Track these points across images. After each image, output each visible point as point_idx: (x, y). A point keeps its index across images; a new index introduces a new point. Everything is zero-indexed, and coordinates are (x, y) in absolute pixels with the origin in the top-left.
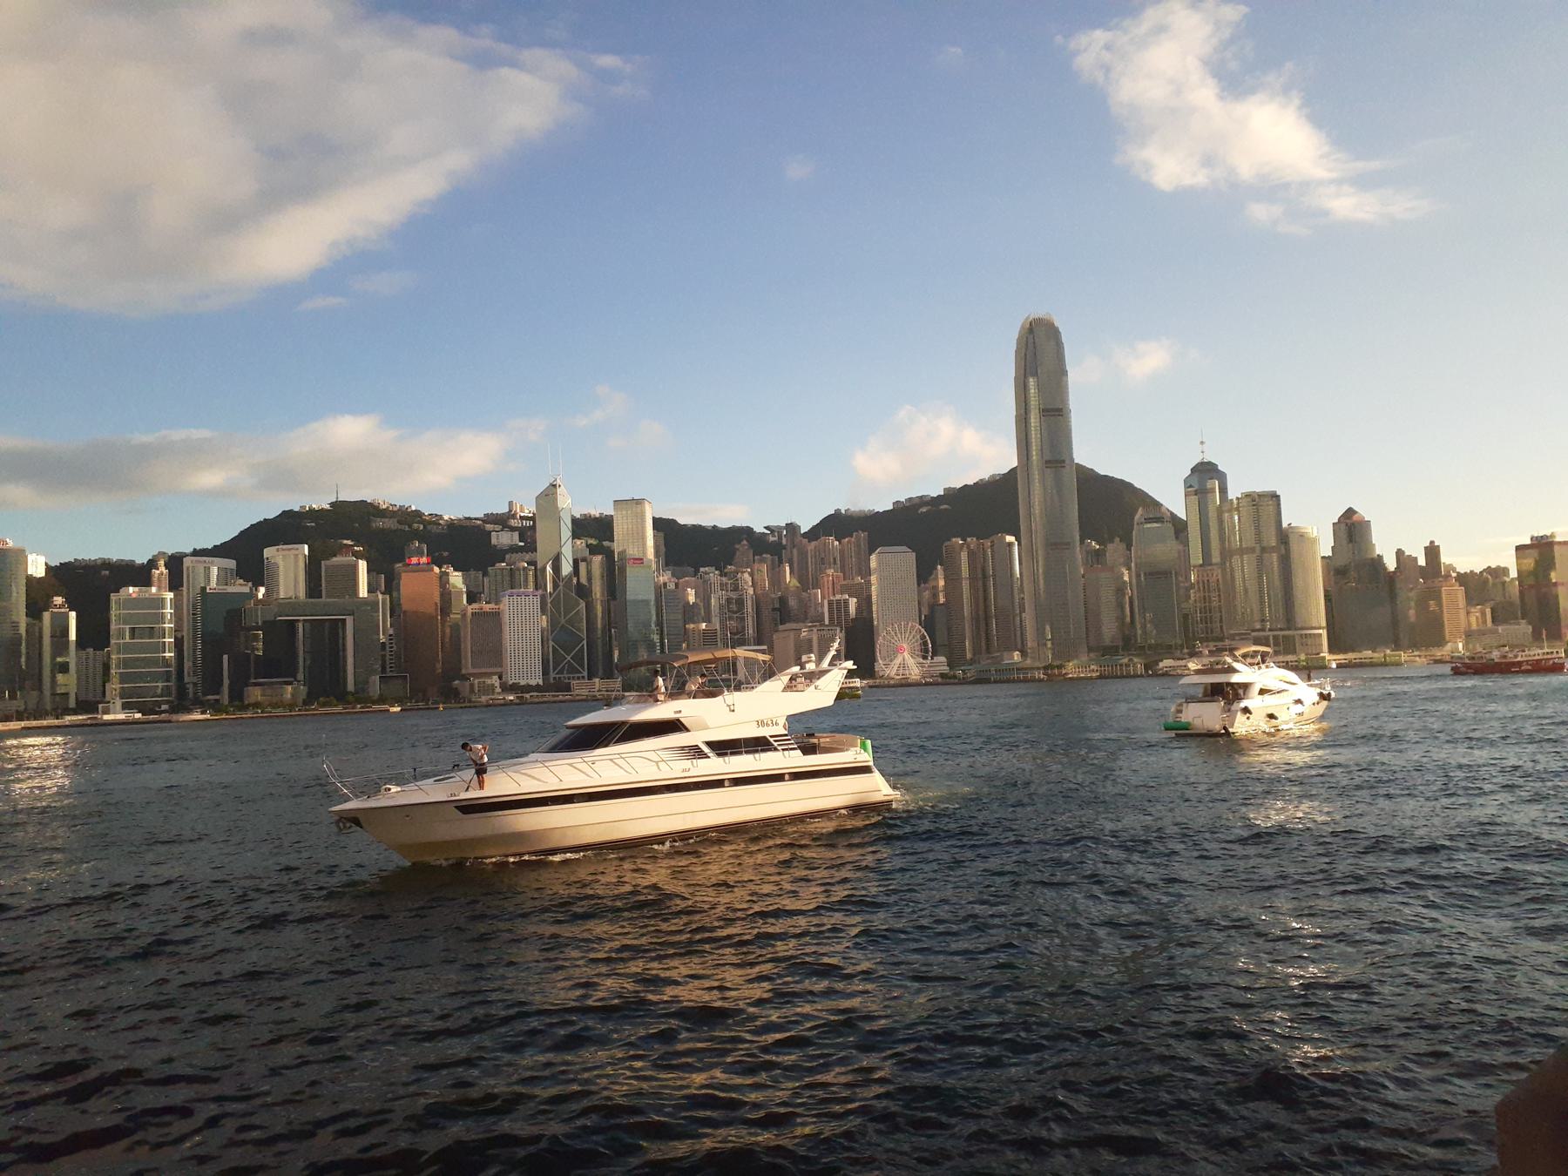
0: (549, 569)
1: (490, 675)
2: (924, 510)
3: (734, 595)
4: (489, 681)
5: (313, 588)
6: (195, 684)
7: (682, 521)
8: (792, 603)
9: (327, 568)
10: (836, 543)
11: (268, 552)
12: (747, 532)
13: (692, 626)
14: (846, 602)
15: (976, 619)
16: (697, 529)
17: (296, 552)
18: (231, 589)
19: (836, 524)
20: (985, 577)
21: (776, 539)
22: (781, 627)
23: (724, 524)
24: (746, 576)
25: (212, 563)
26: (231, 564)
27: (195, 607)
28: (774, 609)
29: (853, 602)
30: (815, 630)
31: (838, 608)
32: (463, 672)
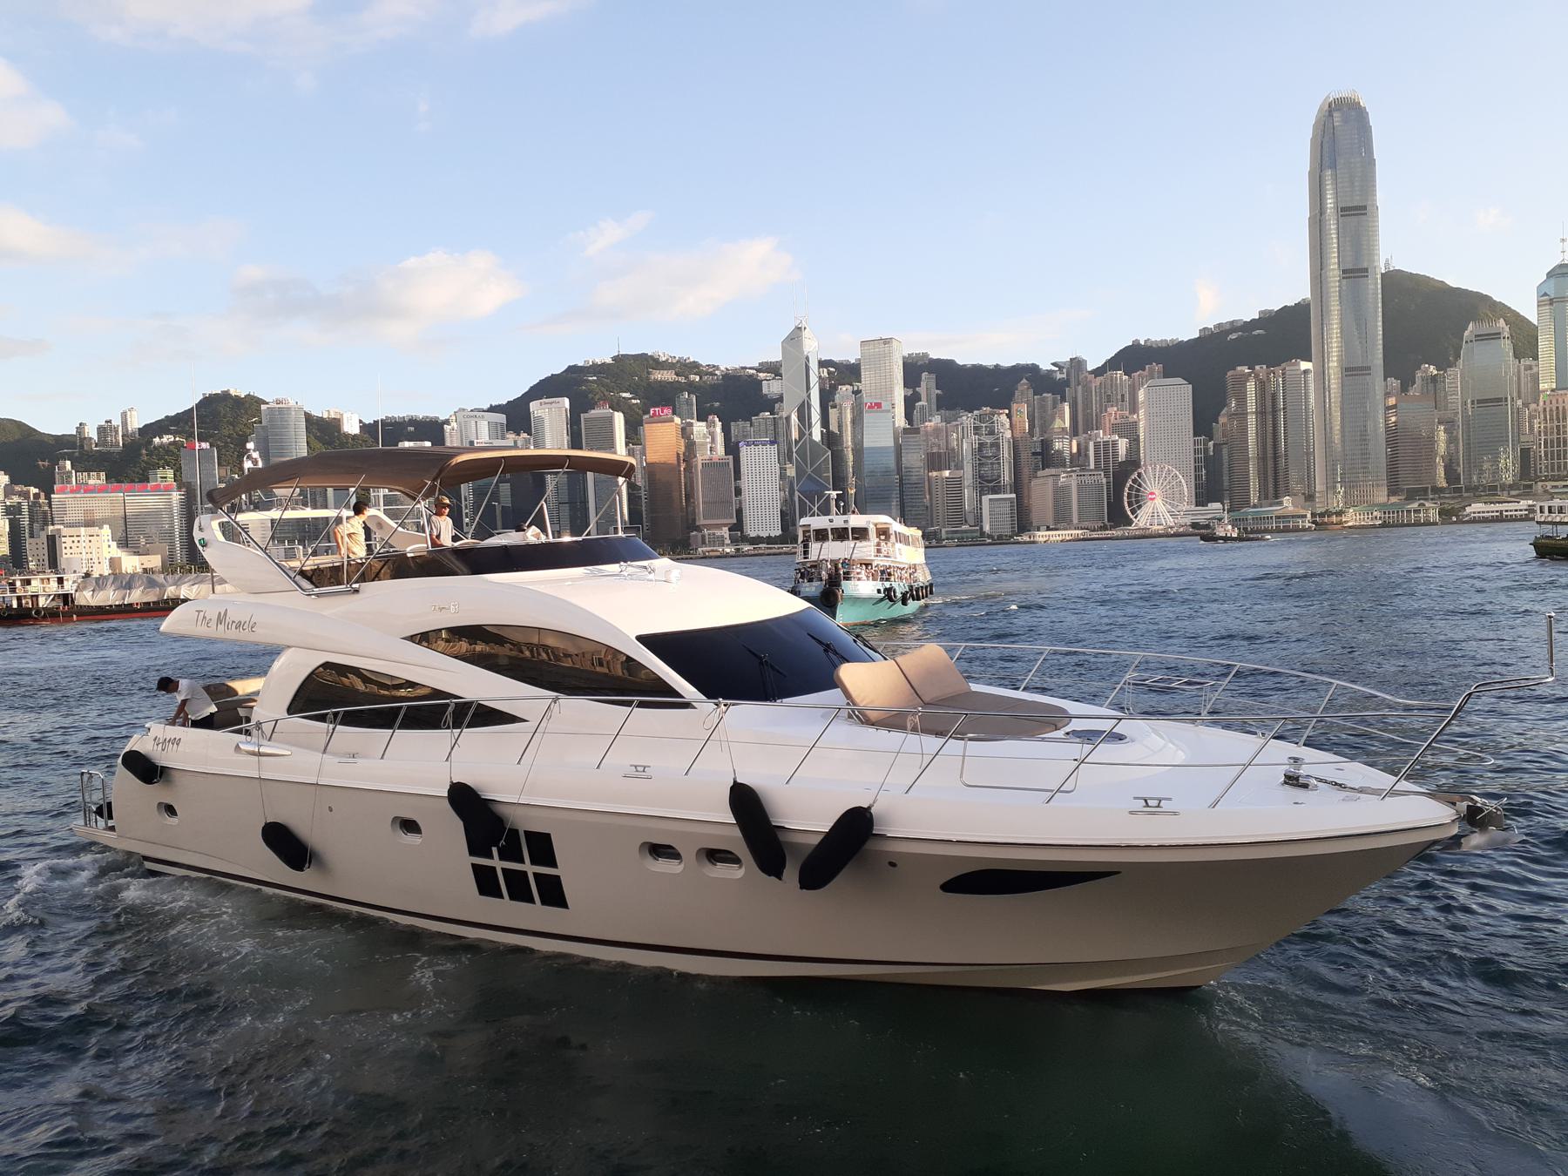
0: (794, 418)
1: (719, 526)
2: (1233, 336)
3: (989, 440)
7: (960, 362)
9: (586, 420)
10: (1125, 377)
12: (1033, 369)
13: (935, 474)
14: (1115, 444)
15: (1262, 458)
16: (978, 370)
19: (1134, 358)
20: (1275, 411)
21: (1064, 376)
22: (1040, 473)
23: (1007, 363)
24: (1004, 418)
28: (1034, 454)
29: (1123, 445)
31: (1106, 449)
32: (697, 524)
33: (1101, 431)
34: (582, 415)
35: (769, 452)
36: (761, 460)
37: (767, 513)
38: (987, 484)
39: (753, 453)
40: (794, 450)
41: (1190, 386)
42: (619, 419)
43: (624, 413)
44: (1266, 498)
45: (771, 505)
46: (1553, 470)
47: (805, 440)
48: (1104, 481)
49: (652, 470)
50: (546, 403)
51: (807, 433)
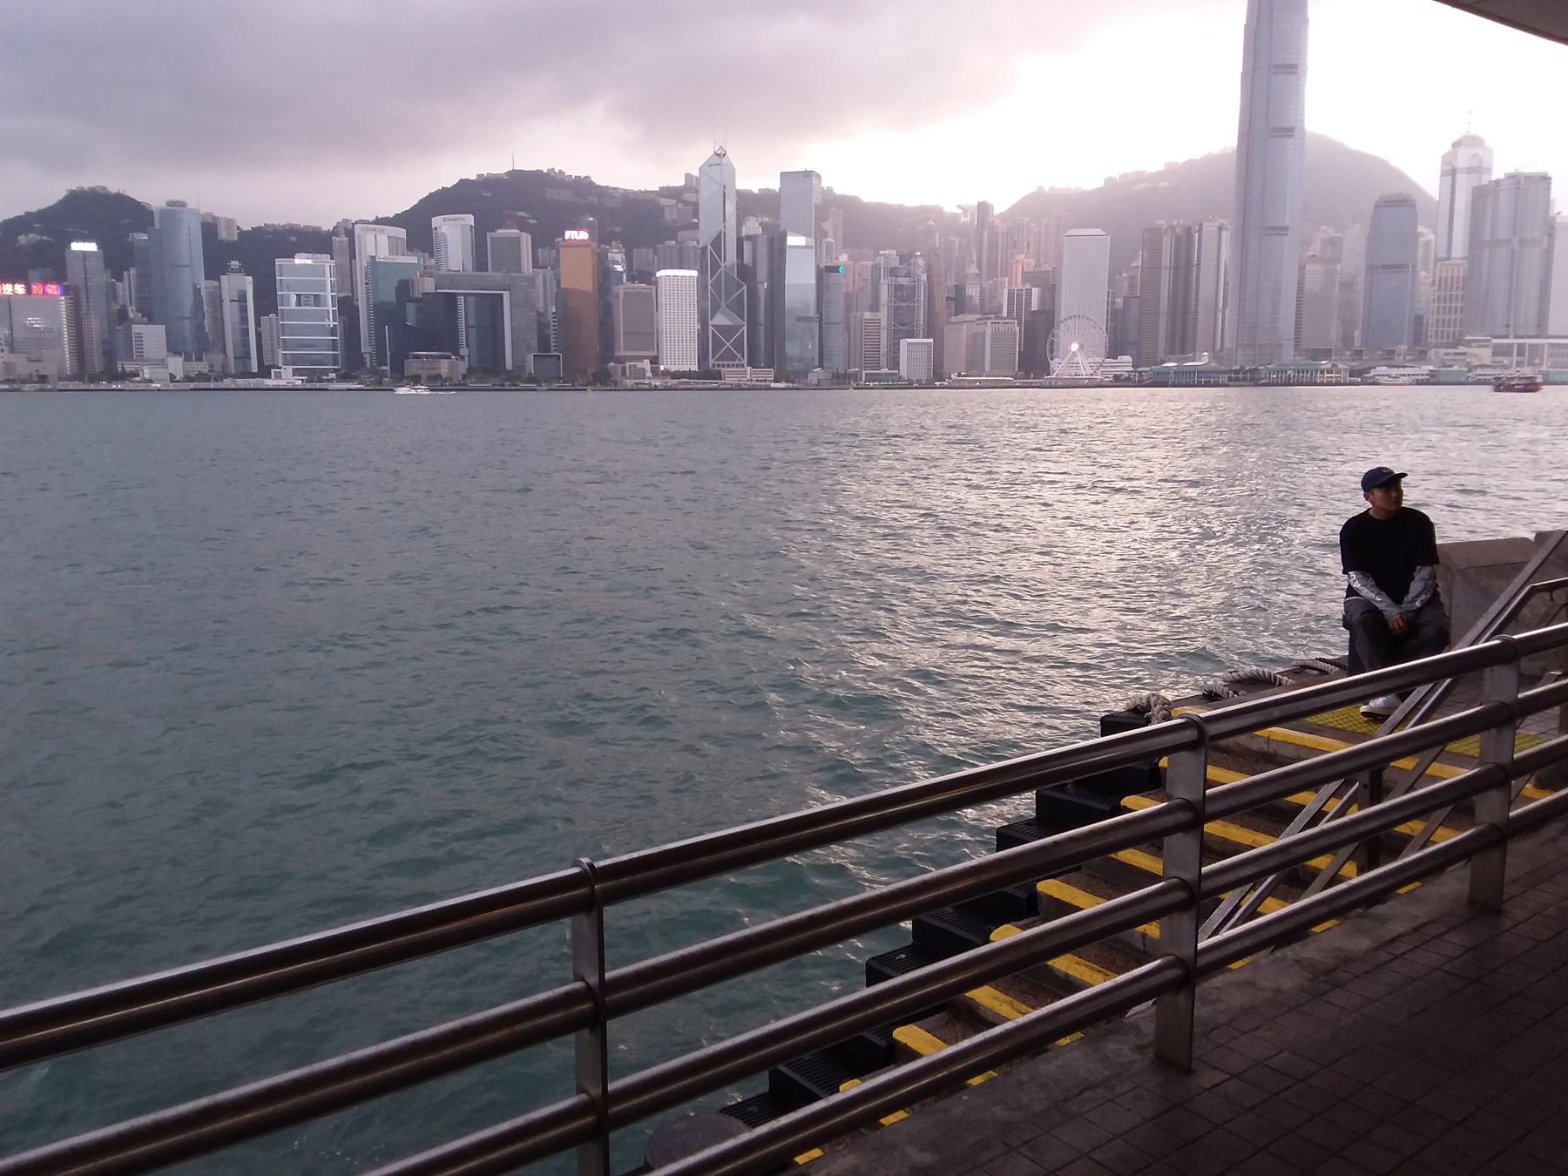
3: (903, 281)
4: (639, 365)
5: (480, 263)
6: (370, 353)
8: (973, 291)
11: (437, 221)
14: (1029, 292)
15: (1172, 312)
17: (463, 222)
18: (401, 259)
22: (954, 319)
25: (383, 231)
26: (401, 233)
27: (366, 275)
28: (947, 299)
29: (1035, 291)
30: (989, 322)
33: (1007, 279)
34: (488, 234)
38: (902, 326)
41: (1109, 237)
42: (526, 240)
44: (1172, 352)
45: (684, 338)
46: (1442, 337)
47: (721, 272)
48: (1018, 329)
49: (563, 297)
51: (723, 265)
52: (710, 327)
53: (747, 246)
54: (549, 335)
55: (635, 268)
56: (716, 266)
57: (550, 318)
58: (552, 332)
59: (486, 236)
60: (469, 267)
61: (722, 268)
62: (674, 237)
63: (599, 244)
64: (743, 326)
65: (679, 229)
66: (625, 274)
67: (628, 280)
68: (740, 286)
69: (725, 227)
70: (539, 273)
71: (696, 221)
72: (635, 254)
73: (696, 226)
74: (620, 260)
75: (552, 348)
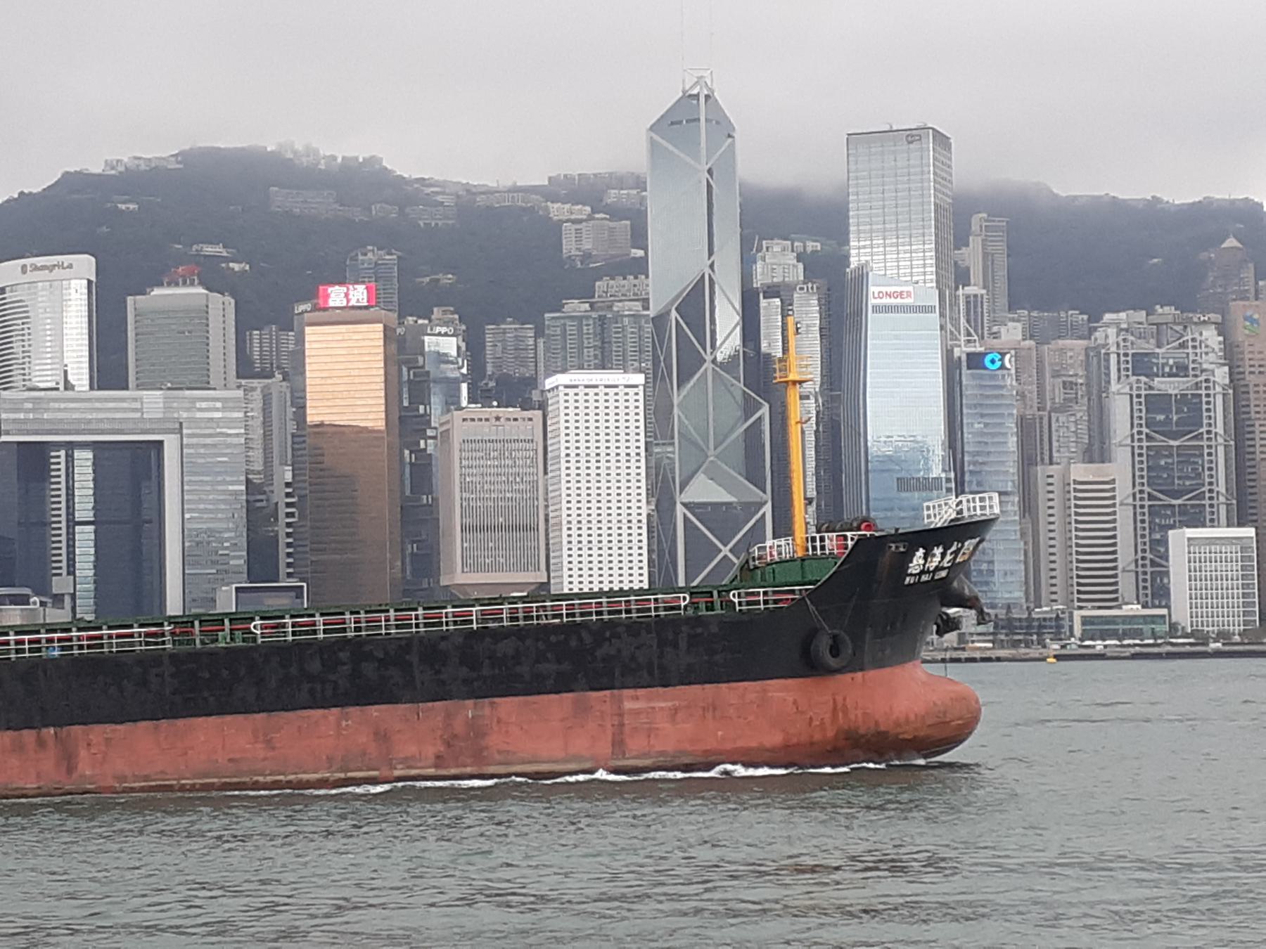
34: (130, 299)
35: (602, 404)
36: (602, 424)
37: (595, 559)
39: (581, 404)
40: (676, 402)
42: (222, 308)
43: (233, 295)
47: (706, 370)
50: (36, 268)
51: (708, 358)
52: (680, 510)
53: (770, 308)
54: (277, 535)
55: (490, 369)
56: (690, 364)
57: (279, 495)
58: (282, 530)
59: (125, 302)
60: (80, 376)
61: (708, 365)
62: (586, 293)
63: (401, 316)
64: (766, 502)
65: (598, 274)
66: (464, 387)
67: (472, 400)
68: (759, 406)
69: (712, 266)
70: (253, 389)
71: (640, 253)
72: (489, 338)
73: (640, 267)
74: (454, 353)
75: (283, 570)
